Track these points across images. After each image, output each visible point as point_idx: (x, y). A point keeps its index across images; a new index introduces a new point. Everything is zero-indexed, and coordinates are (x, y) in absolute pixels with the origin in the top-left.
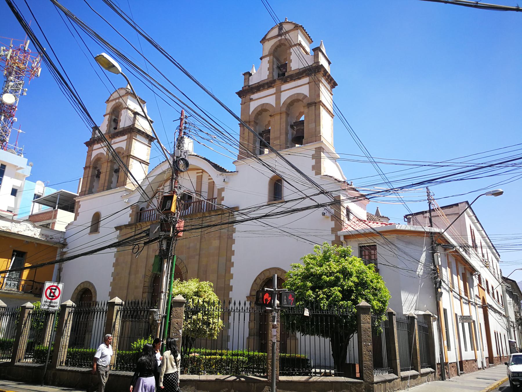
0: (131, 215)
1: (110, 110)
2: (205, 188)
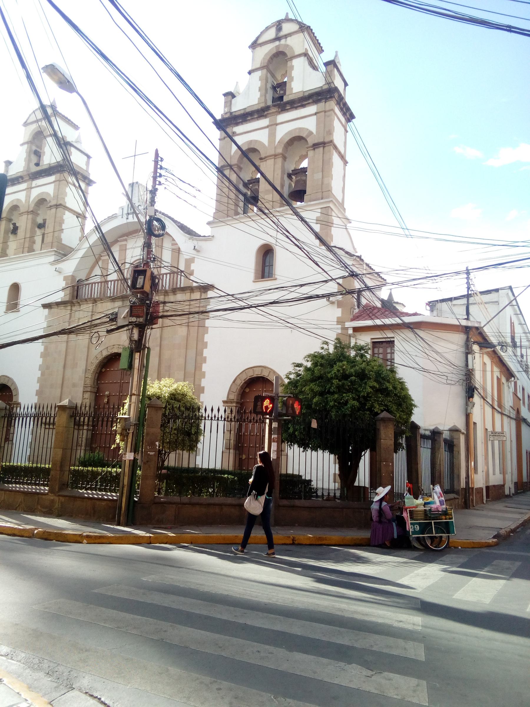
2: (167, 256)
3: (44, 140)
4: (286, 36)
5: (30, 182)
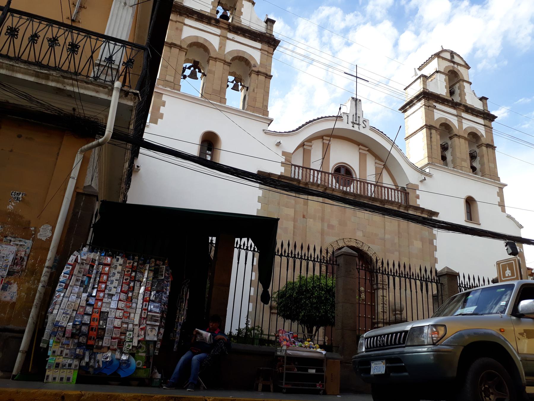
4: (458, 64)
5: (225, 32)
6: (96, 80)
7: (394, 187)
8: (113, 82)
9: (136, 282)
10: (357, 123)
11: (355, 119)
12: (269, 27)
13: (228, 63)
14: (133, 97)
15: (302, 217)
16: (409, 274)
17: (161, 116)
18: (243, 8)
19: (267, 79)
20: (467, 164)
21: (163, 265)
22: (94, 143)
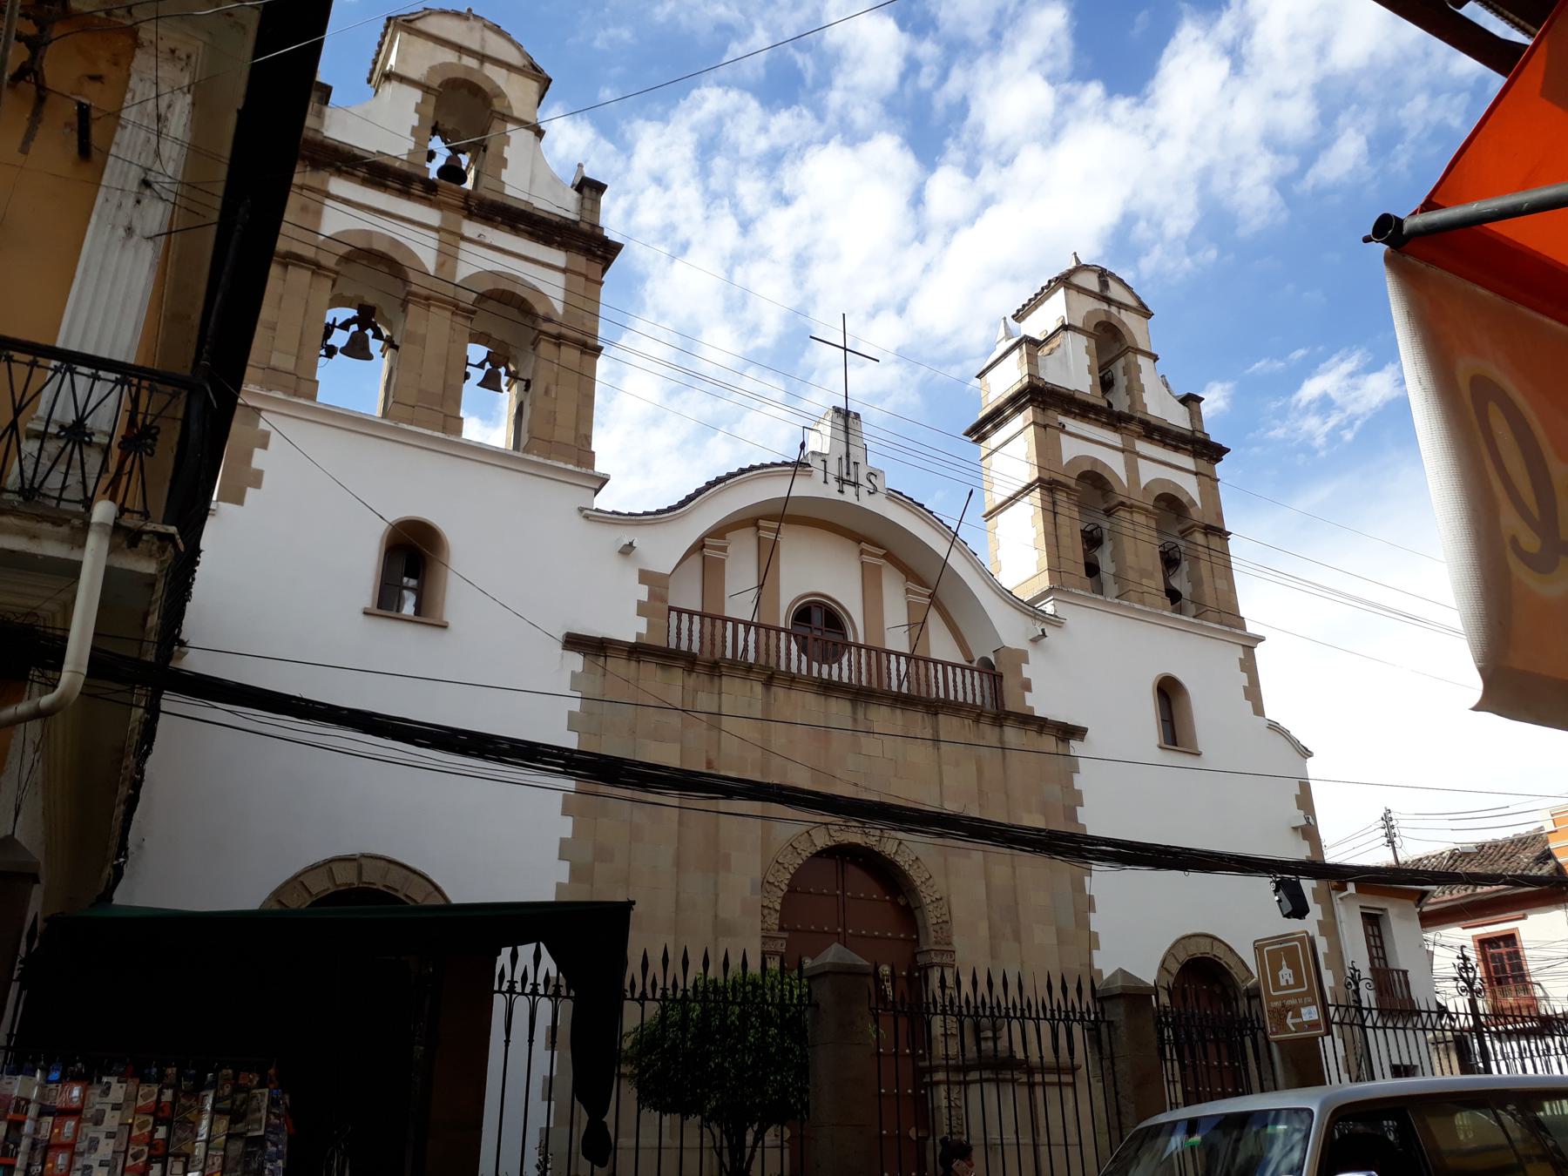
0: (642, 609)
1: (425, 72)
3: (496, 124)
4: (1121, 306)
5: (453, 216)
6: (27, 499)
7: (959, 659)
8: (88, 503)
9: (170, 1159)
10: (853, 480)
11: (845, 471)
12: (588, 204)
13: (464, 310)
14: (154, 547)
15: (705, 765)
16: (1019, 1007)
17: (256, 479)
18: (509, 145)
19: (587, 358)
20: (1156, 582)
21: (261, 1085)
22: (23, 708)
